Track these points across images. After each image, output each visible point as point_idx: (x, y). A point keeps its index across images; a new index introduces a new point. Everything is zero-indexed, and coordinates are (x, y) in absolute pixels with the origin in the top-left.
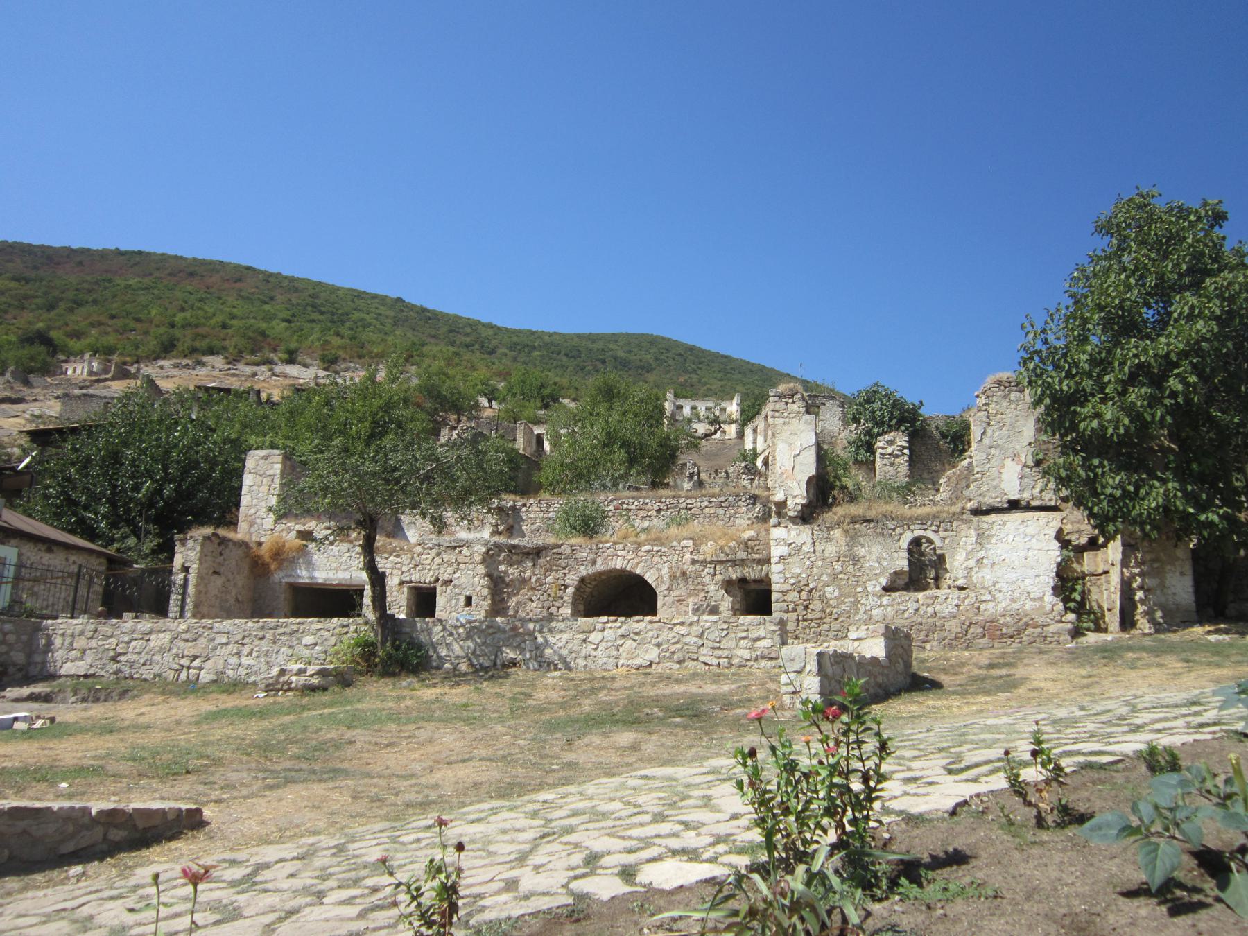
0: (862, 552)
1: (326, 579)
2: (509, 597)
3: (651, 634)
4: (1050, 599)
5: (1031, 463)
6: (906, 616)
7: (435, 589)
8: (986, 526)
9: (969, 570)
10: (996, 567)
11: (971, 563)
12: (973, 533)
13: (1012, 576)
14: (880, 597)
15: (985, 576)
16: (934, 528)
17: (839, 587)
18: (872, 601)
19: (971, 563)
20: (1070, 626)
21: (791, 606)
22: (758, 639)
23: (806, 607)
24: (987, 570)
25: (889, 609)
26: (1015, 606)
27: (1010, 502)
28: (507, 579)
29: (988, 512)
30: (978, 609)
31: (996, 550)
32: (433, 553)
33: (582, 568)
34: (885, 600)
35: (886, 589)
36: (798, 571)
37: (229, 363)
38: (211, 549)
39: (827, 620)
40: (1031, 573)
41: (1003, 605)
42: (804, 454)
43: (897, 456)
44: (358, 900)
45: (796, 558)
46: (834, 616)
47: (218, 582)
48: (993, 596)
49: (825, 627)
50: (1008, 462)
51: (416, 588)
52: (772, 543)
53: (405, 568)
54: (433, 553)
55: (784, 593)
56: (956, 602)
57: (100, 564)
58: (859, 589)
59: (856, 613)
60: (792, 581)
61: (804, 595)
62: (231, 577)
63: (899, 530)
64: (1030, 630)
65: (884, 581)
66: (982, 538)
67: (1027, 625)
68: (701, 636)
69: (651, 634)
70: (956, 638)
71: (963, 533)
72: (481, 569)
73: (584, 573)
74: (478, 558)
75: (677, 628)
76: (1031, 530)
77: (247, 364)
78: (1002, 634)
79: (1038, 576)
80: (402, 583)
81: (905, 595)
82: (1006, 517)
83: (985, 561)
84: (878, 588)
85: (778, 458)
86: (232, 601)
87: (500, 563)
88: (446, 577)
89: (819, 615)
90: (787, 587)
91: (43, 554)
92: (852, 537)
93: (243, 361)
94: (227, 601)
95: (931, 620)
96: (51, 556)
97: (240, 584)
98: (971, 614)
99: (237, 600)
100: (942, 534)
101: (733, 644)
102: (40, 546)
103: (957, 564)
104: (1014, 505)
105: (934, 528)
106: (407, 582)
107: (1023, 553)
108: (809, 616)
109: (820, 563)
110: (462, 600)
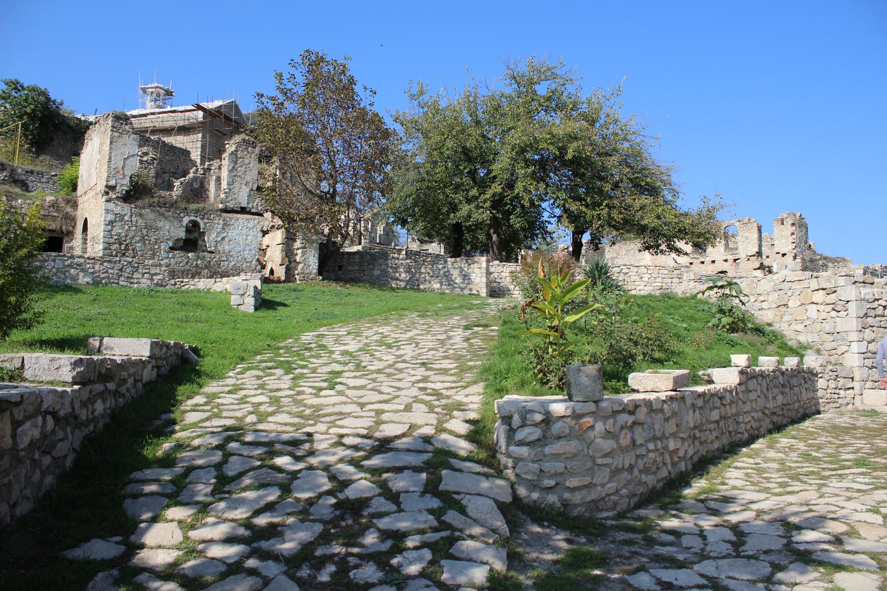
3: (88, 266)
5: (255, 188)
13: (238, 249)
14: (169, 252)
21: (114, 253)
22: (156, 274)
27: (241, 208)
29: (232, 211)
31: (232, 233)
34: (171, 255)
35: (172, 249)
41: (233, 263)
43: (149, 164)
44: (227, 389)
45: (119, 224)
50: (244, 186)
60: (116, 237)
61: (123, 247)
66: (226, 225)
68: (121, 270)
69: (88, 266)
71: (216, 222)
75: (105, 264)
76: (251, 225)
81: (182, 253)
82: (239, 216)
90: (112, 241)
100: (206, 221)
101: (140, 276)
103: (210, 239)
104: (243, 211)
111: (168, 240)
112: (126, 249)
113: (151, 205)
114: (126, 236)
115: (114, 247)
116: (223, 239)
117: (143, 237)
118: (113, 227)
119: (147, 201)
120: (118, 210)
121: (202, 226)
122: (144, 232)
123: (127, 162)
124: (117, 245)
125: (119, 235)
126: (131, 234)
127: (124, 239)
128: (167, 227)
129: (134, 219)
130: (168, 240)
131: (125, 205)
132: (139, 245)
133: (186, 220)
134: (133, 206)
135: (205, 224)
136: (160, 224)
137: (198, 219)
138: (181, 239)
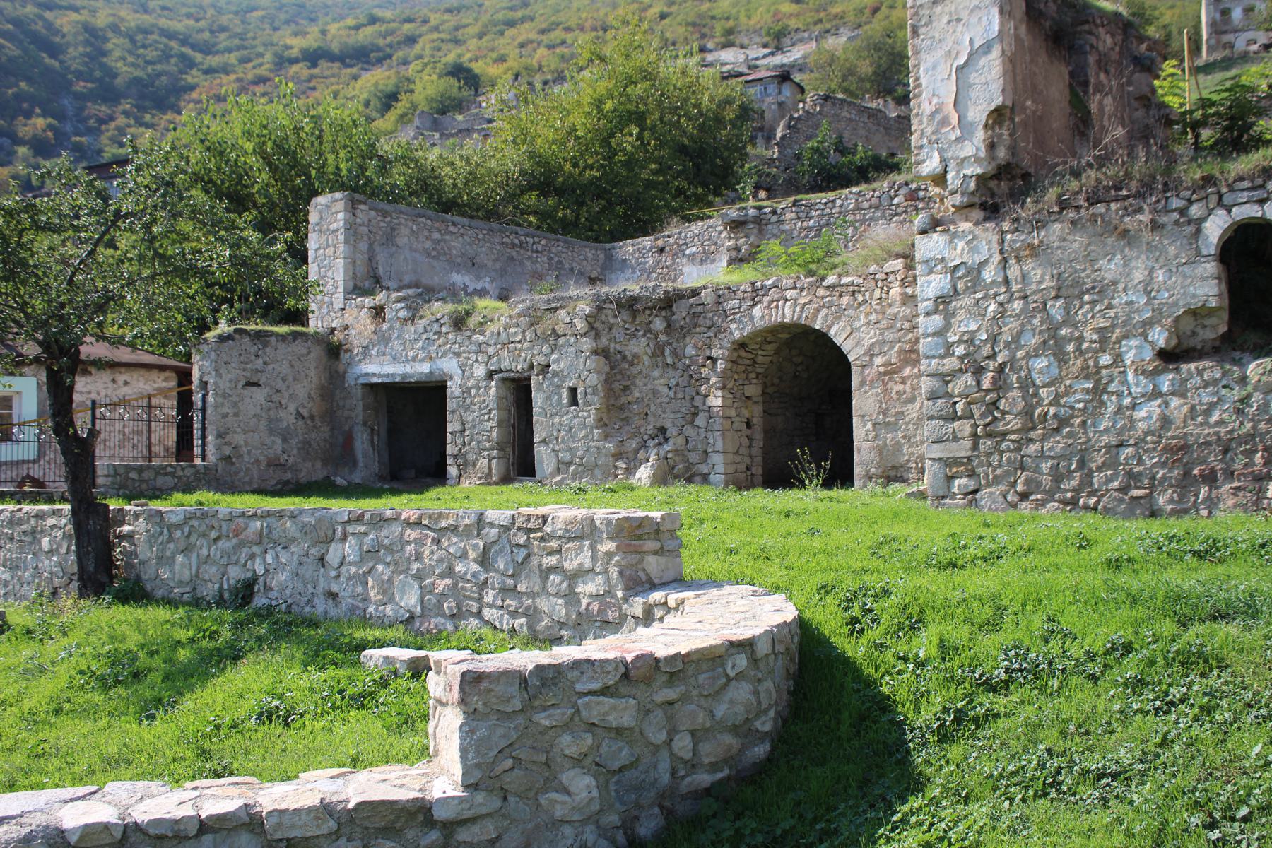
7: (529, 379)
14: (1156, 372)
21: (960, 407)
23: (994, 403)
25: (1175, 402)
35: (1169, 357)
36: (973, 327)
45: (967, 301)
47: (259, 395)
49: (1033, 448)
51: (504, 380)
53: (491, 350)
57: (166, 380)
58: (1105, 359)
60: (960, 350)
62: (280, 385)
63: (1195, 211)
65: (1160, 337)
73: (737, 335)
74: (580, 325)
80: (490, 375)
81: (1210, 369)
84: (1148, 354)
85: (924, 81)
86: (292, 419)
88: (542, 360)
90: (951, 364)
94: (279, 420)
96: (89, 379)
99: (299, 415)
106: (496, 372)
108: (1001, 426)
109: (1017, 305)
110: (565, 393)
111: (1148, 324)
112: (1000, 385)
113: (1063, 205)
114: (993, 339)
115: (957, 386)
117: (1053, 329)
118: (949, 316)
119: (1052, 194)
120: (958, 253)
122: (1056, 310)
123: (973, 77)
124: (968, 378)
125: (969, 340)
126: (1009, 328)
127: (986, 350)
128: (1138, 275)
129: (1014, 271)
130: (1148, 324)
131: (978, 231)
132: (1040, 363)
133: (1215, 227)
134: (1006, 226)
136: (1110, 268)
138: (1211, 312)
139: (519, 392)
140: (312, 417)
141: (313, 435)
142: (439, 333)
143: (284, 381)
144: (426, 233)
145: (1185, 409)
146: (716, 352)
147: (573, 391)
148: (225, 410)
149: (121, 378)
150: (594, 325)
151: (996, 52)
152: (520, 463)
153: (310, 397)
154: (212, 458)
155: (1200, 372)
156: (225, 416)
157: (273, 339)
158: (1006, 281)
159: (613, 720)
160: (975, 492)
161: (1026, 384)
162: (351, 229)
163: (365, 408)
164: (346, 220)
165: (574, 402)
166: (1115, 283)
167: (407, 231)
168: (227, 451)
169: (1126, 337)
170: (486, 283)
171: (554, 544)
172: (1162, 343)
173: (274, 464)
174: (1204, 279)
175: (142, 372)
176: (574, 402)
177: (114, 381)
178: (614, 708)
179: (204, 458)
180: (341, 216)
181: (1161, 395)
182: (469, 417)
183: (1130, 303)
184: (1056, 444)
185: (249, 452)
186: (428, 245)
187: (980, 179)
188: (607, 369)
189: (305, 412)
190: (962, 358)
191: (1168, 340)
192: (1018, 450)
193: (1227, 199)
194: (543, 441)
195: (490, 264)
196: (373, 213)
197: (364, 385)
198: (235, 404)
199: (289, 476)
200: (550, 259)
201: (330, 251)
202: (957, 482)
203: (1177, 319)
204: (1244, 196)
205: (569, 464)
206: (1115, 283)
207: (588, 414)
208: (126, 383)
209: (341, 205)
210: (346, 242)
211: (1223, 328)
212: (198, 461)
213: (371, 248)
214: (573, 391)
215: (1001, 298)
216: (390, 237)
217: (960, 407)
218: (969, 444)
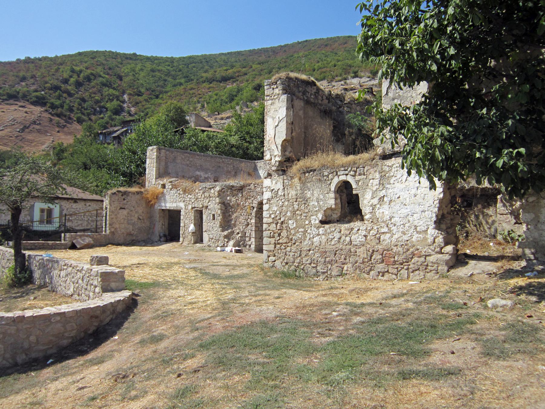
0: (309, 194)
1: (170, 207)
2: (233, 214)
4: (432, 232)
6: (333, 243)
8: (387, 169)
9: (373, 207)
10: (393, 204)
11: (375, 201)
12: (377, 175)
13: (404, 211)
14: (318, 228)
15: (384, 211)
16: (352, 173)
17: (296, 221)
18: (314, 231)
19: (375, 201)
20: (447, 257)
24: (386, 206)
25: (323, 237)
26: (405, 238)
28: (231, 204)
30: (379, 239)
32: (201, 191)
33: (259, 197)
34: (321, 231)
35: (323, 222)
37: (329, 83)
38: (117, 198)
39: (290, 244)
40: (418, 209)
41: (396, 236)
42: (280, 124)
46: (293, 242)
47: (125, 212)
48: (389, 229)
51: (197, 210)
52: (264, 190)
54: (201, 191)
55: (269, 224)
56: (364, 233)
59: (305, 240)
60: (273, 216)
62: (132, 209)
64: (415, 259)
65: (320, 216)
67: (413, 254)
70: (363, 262)
72: (218, 200)
77: (336, 82)
78: (395, 261)
79: (423, 211)
80: (193, 208)
83: (385, 199)
84: (317, 222)
86: (136, 220)
87: (228, 196)
89: (285, 241)
90: (270, 220)
91: (72, 204)
92: (303, 183)
93: (335, 80)
94: (132, 220)
95: (348, 247)
96: (77, 204)
97: (140, 211)
98: (374, 243)
99: (139, 219)
102: (70, 201)
103: (366, 203)
105: (352, 173)
107: (414, 191)
108: (281, 241)
109: (286, 203)
110: (211, 216)
116: (382, 199)
121: (354, 186)
124: (274, 225)
127: (278, 218)
129: (286, 193)
135: (357, 182)
137: (350, 179)
139: (199, 214)
140: (143, 220)
141: (144, 225)
142: (179, 194)
143: (134, 207)
144: (187, 158)
145: (326, 239)
146: (254, 205)
147: (214, 215)
148: (112, 217)
149: (88, 204)
150: (221, 193)
151: (285, 122)
152: (198, 237)
153: (143, 212)
154: (108, 232)
155: (330, 228)
156: (113, 218)
157: (130, 194)
158: (284, 195)
159: (9, 331)
160: (275, 261)
161: (288, 229)
162: (158, 158)
163: (160, 217)
164: (157, 155)
165: (214, 219)
166: (310, 198)
167: (180, 158)
168: (113, 230)
169: (312, 216)
170: (209, 175)
171: (92, 277)
172: (320, 219)
173: (130, 234)
174: (331, 198)
175: (95, 202)
176: (214, 219)
177: (85, 205)
178: (9, 329)
179: (105, 231)
180: (155, 154)
181: (320, 235)
182: (186, 222)
183: (313, 205)
184: (294, 248)
185: (120, 230)
186: (188, 162)
187: (279, 161)
188: (224, 209)
189: (141, 217)
190: (273, 218)
191: (322, 218)
192: (285, 249)
193: (339, 173)
194: (205, 231)
195: (211, 168)
196: (168, 152)
197: (160, 209)
198: (116, 215)
199: (134, 238)
200: (234, 166)
201: (152, 165)
202: (270, 258)
203: (325, 211)
204: (342, 173)
205: (212, 239)
206: (310, 198)
207: (217, 223)
208: (89, 206)
209: (155, 150)
210: (156, 162)
211: (339, 214)
212: (104, 233)
213: (166, 164)
214: (214, 215)
215: (283, 200)
216: (175, 159)
217: (272, 234)
218: (273, 246)
